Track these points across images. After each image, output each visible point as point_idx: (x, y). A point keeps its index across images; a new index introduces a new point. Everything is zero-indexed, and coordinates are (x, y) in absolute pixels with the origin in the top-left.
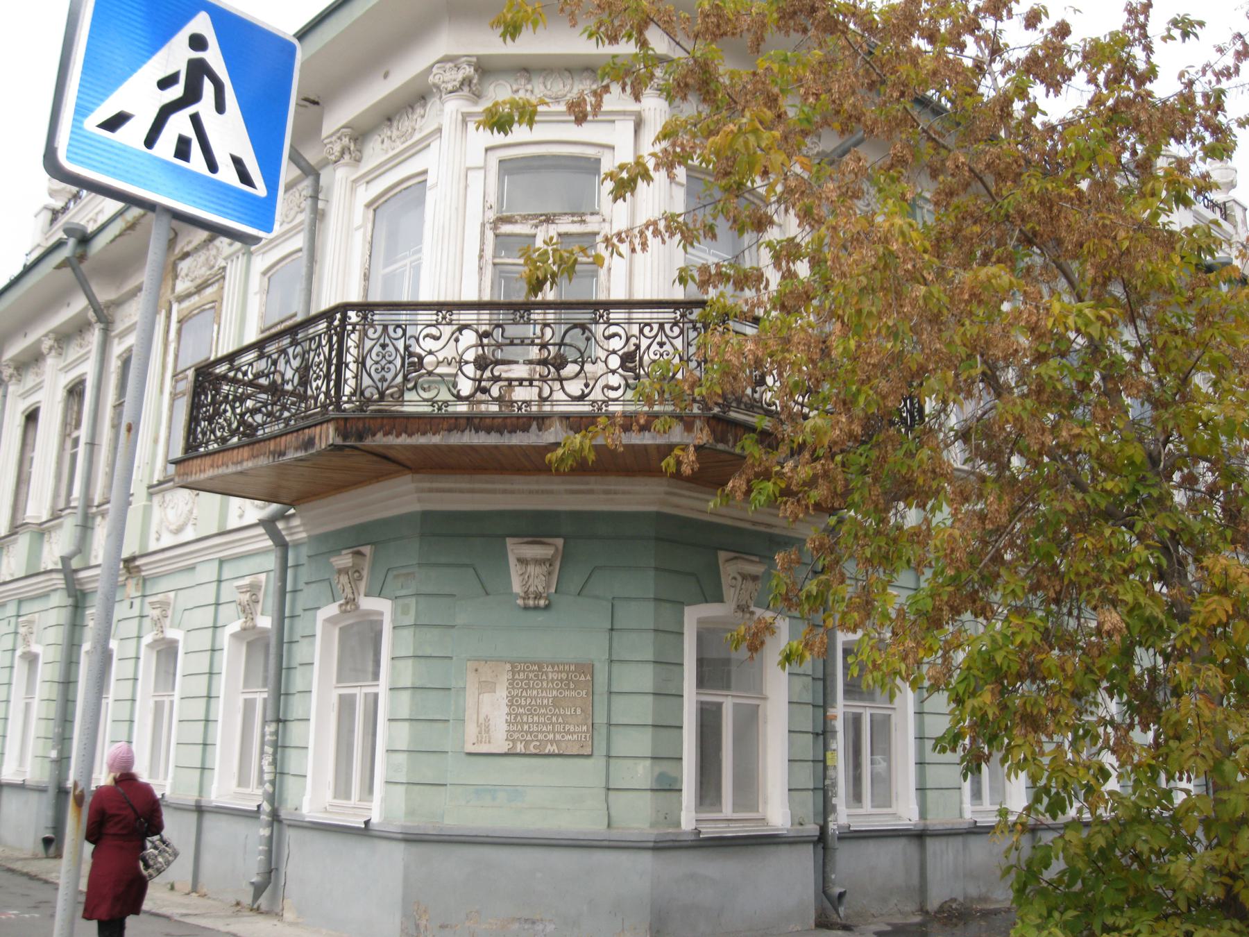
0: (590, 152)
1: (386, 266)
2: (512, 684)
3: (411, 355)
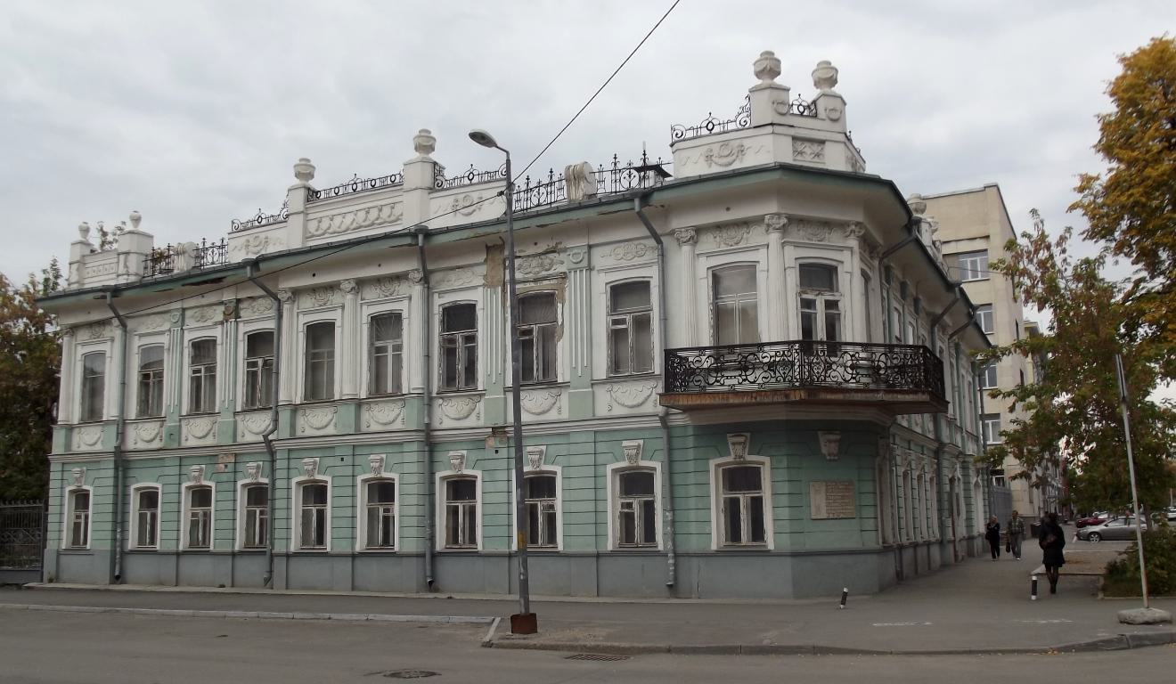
0: (834, 263)
2: (827, 490)
3: (828, 363)
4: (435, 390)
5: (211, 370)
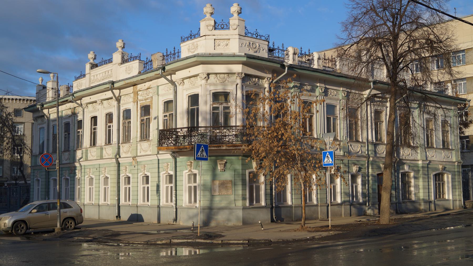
1: (191, 107)
4: (120, 142)
5: (69, 134)
